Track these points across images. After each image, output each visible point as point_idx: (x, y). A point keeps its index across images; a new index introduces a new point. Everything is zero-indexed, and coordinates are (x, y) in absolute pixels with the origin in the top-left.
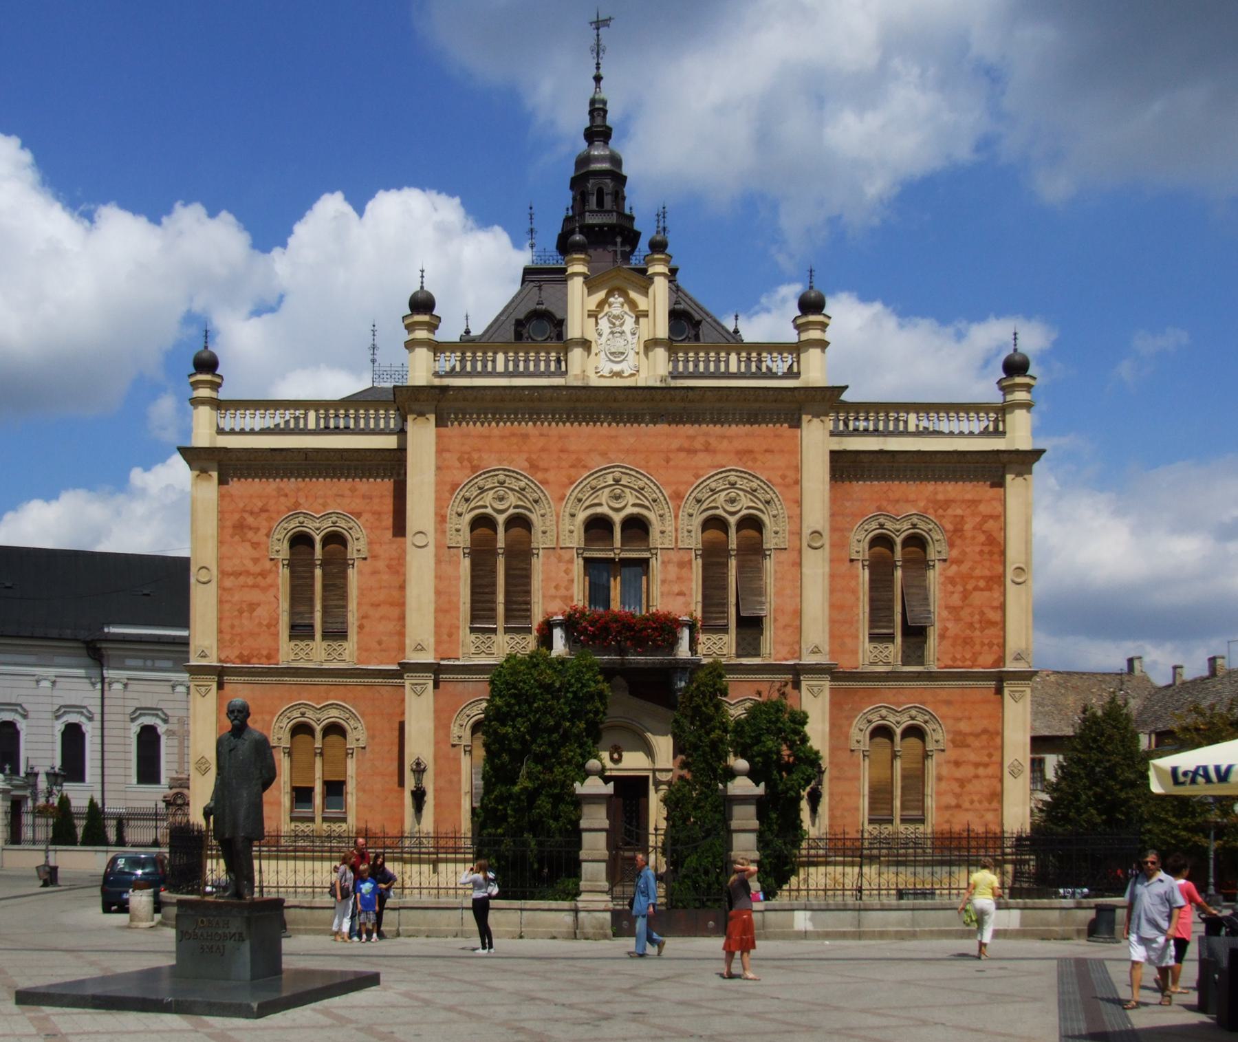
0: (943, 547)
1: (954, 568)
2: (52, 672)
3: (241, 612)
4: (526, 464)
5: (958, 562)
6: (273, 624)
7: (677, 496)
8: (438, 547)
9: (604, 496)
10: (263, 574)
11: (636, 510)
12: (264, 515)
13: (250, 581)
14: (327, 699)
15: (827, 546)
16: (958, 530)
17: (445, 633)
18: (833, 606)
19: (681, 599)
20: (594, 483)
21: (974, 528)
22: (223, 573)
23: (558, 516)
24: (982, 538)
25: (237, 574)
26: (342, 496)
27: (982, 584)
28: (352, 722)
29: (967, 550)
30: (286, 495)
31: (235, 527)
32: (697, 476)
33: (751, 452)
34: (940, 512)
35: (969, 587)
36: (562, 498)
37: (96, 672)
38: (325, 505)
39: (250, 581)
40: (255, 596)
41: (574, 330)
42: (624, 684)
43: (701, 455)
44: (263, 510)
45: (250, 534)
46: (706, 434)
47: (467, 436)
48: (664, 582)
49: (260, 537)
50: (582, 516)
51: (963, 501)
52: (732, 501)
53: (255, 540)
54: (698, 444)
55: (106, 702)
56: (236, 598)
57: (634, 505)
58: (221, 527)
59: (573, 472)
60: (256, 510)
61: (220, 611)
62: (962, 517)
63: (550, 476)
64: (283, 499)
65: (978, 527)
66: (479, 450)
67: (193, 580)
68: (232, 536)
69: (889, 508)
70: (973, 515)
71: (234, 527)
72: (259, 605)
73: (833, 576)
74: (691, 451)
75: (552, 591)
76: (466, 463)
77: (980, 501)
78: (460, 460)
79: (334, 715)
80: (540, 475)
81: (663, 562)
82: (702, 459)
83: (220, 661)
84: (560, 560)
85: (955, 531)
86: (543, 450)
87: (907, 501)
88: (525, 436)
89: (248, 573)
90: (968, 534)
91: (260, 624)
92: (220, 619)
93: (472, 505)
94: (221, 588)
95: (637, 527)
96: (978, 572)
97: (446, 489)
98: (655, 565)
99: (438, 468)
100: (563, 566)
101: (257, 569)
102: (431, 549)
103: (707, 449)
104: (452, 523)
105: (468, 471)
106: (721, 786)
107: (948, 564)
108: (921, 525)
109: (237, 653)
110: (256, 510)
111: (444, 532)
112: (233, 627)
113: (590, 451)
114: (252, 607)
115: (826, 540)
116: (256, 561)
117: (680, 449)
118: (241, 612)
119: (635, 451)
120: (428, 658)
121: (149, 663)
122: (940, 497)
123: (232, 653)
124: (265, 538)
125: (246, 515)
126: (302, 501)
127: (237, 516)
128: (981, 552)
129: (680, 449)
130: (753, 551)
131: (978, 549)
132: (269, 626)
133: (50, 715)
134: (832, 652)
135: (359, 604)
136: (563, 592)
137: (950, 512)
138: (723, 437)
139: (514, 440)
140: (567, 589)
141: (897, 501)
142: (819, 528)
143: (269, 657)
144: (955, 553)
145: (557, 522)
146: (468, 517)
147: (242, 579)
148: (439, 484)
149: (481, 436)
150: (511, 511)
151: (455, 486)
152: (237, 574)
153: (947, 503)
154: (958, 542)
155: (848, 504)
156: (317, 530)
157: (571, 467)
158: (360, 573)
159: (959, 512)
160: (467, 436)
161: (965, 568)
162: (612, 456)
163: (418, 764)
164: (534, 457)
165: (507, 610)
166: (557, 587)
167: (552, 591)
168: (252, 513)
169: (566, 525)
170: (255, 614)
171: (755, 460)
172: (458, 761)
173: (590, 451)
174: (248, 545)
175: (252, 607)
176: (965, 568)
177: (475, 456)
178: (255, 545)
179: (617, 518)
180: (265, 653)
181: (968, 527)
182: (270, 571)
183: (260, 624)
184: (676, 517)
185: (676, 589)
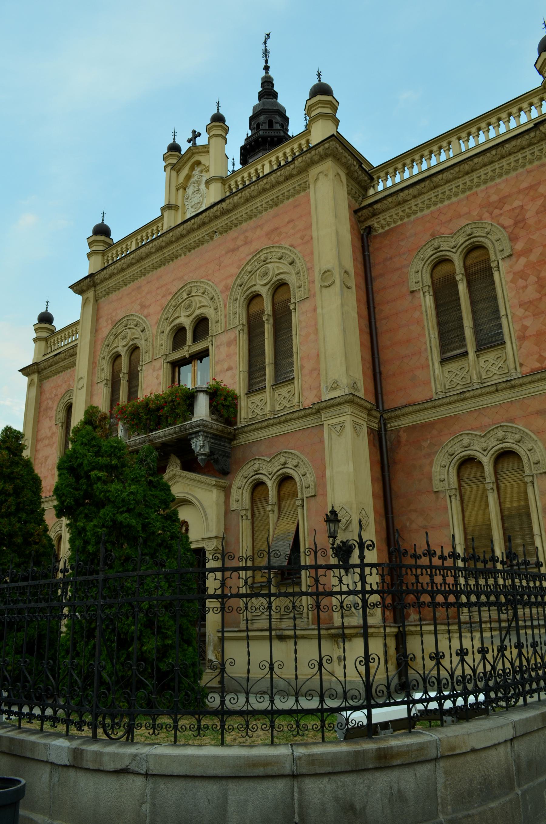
0: (506, 245)
1: (523, 261)
5: (526, 252)
16: (520, 222)
20: (174, 303)
21: (537, 213)
29: (534, 237)
33: (277, 229)
34: (497, 212)
42: (179, 462)
57: (199, 308)
62: (522, 207)
69: (443, 230)
70: (533, 199)
74: (234, 250)
77: (539, 184)
85: (516, 224)
87: (460, 216)
90: (531, 222)
103: (246, 243)
107: (514, 259)
137: (507, 208)
144: (519, 246)
153: (502, 201)
157: (163, 297)
159: (517, 203)
161: (533, 257)
176: (533, 257)
185: (226, 366)
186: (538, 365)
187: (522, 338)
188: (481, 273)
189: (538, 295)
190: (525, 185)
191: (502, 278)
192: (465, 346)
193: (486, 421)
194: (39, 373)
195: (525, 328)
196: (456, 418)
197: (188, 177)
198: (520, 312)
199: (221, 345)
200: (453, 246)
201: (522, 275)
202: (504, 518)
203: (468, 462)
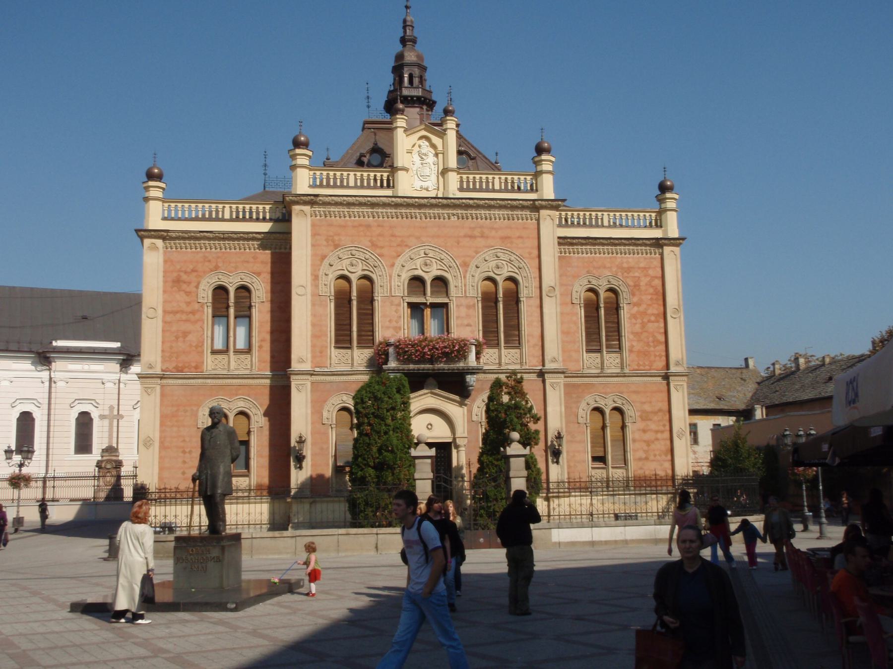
1: (636, 309)
3: (177, 338)
4: (370, 244)
6: (200, 344)
7: (466, 265)
8: (313, 295)
9: (419, 262)
10: (193, 313)
11: (439, 273)
12: (195, 274)
13: (184, 317)
14: (237, 395)
15: (558, 296)
16: (637, 286)
17: (318, 352)
18: (563, 332)
19: (469, 329)
21: (646, 285)
22: (165, 312)
23: (391, 277)
24: (651, 290)
25: (175, 313)
26: (248, 262)
27: (653, 318)
28: (254, 410)
29: (643, 297)
30: (209, 261)
31: (176, 281)
32: (477, 253)
35: (645, 320)
36: (393, 265)
38: (236, 268)
39: (184, 317)
40: (188, 327)
42: (435, 383)
43: (479, 240)
44: (193, 271)
45: (184, 286)
46: (481, 227)
47: (331, 225)
48: (458, 317)
49: (192, 288)
50: (406, 276)
51: (639, 268)
53: (188, 290)
54: (477, 232)
56: (174, 329)
58: (165, 282)
59: (399, 249)
60: (189, 270)
61: (163, 337)
63: (385, 251)
64: (207, 264)
65: (649, 284)
66: (339, 235)
67: (144, 316)
68: (172, 287)
69: (594, 271)
70: (646, 276)
71: (173, 281)
72: (190, 333)
73: (562, 314)
74: (472, 237)
75: (387, 324)
76: (330, 242)
77: (649, 268)
78: (327, 240)
79: (241, 405)
80: (378, 251)
81: (457, 306)
82: (480, 242)
83: (163, 370)
84: (392, 304)
85: (635, 286)
86: (380, 235)
87: (605, 267)
88: (368, 226)
89: (182, 312)
90: (643, 288)
91: (191, 346)
92: (163, 342)
94: (164, 322)
95: (441, 282)
96: (650, 311)
97: (319, 258)
98: (453, 307)
99: (313, 245)
100: (394, 308)
101: (189, 309)
102: (309, 297)
104: (323, 280)
105: (332, 248)
106: (502, 449)
108: (613, 281)
109: (174, 365)
110: (189, 270)
111: (317, 286)
112: (171, 347)
113: (410, 236)
114: (185, 334)
115: (557, 292)
116: (188, 304)
117: (465, 236)
118: (177, 338)
119: (438, 236)
120: (307, 367)
121: (86, 367)
122: (625, 265)
123: (171, 366)
124: (195, 289)
125: (182, 274)
126: (220, 265)
127: (175, 274)
128: (651, 299)
129: (465, 236)
130: (513, 299)
131: (649, 297)
132: (197, 347)
133: (9, 406)
134: (564, 361)
135: (259, 332)
136: (394, 324)
137: (631, 274)
138: (492, 228)
139: (361, 229)
140: (397, 322)
141: (599, 268)
142: (553, 285)
143: (196, 367)
144: (635, 299)
145: (390, 280)
146: (332, 276)
147: (178, 316)
148: (314, 255)
149: (340, 226)
151: (324, 257)
152: (175, 313)
153: (629, 269)
154: (637, 293)
155: (569, 269)
156: (232, 284)
158: (260, 311)
159: (637, 274)
160: (331, 225)
162: (424, 239)
163: (300, 437)
164: (374, 239)
165: (359, 336)
166: (390, 321)
167: (387, 324)
168: (186, 272)
169: (395, 282)
170: (187, 339)
171: (512, 243)
172: (326, 434)
173: (410, 236)
174: (182, 293)
175: (185, 334)
176: (642, 308)
177: (336, 238)
178: (188, 293)
179: (428, 278)
180: (193, 364)
181: (642, 284)
182: (198, 311)
183: (191, 346)
184: (465, 277)
185: (466, 322)
186: (636, 367)
187: (631, 351)
188: (615, 308)
189: (640, 330)
190: (642, 265)
191: (625, 313)
192: (601, 345)
193: (608, 390)
195: (632, 346)
196: (592, 385)
198: (631, 337)
199: (461, 305)
200: (602, 287)
201: (634, 316)
202: (612, 441)
203: (598, 410)
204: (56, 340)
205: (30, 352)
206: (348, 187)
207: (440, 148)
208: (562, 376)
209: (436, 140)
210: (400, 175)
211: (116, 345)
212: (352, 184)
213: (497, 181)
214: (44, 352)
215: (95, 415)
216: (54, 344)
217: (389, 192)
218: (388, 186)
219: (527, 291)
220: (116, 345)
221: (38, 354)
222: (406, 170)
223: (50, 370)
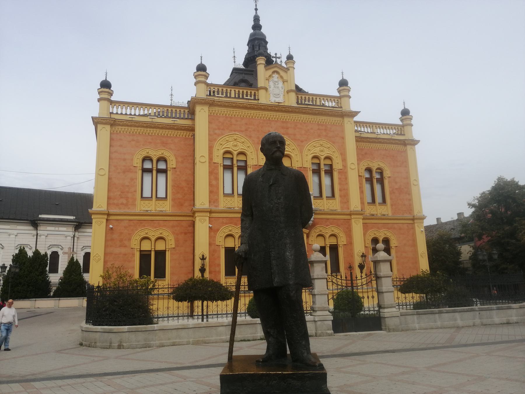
2: (15, 232)
37: (35, 232)
41: (261, 82)
52: (322, 151)
55: (38, 243)
93: (224, 147)
121: (57, 229)
133: (13, 248)
146: (222, 151)
150: (240, 150)
156: (155, 154)
194: (112, 125)
197: (270, 76)
204: (41, 214)
205: (27, 220)
206: (230, 97)
207: (285, 78)
208: (361, 217)
209: (282, 73)
210: (262, 93)
211: (72, 218)
212: (233, 95)
213: (318, 100)
214: (34, 220)
215: (60, 253)
216: (40, 216)
217: (256, 102)
218: (255, 99)
219: (337, 165)
220: (72, 218)
221: (30, 221)
222: (266, 89)
223: (37, 230)
